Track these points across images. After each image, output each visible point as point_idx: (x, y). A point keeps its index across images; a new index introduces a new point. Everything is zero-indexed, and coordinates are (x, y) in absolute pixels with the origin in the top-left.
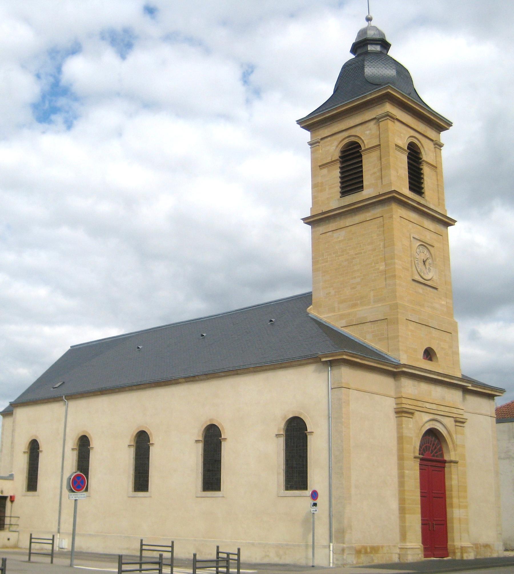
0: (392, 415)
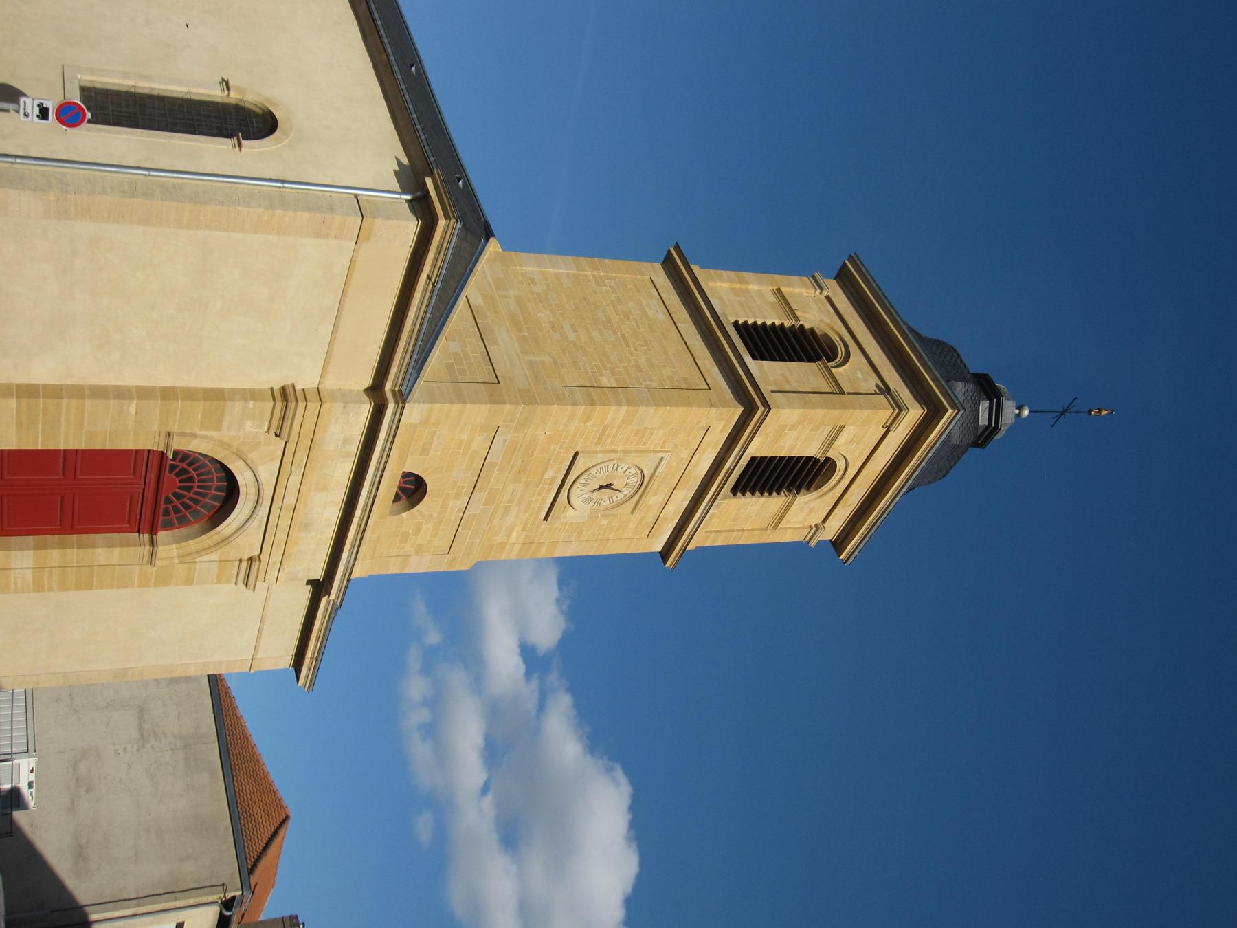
0: (276, 380)
